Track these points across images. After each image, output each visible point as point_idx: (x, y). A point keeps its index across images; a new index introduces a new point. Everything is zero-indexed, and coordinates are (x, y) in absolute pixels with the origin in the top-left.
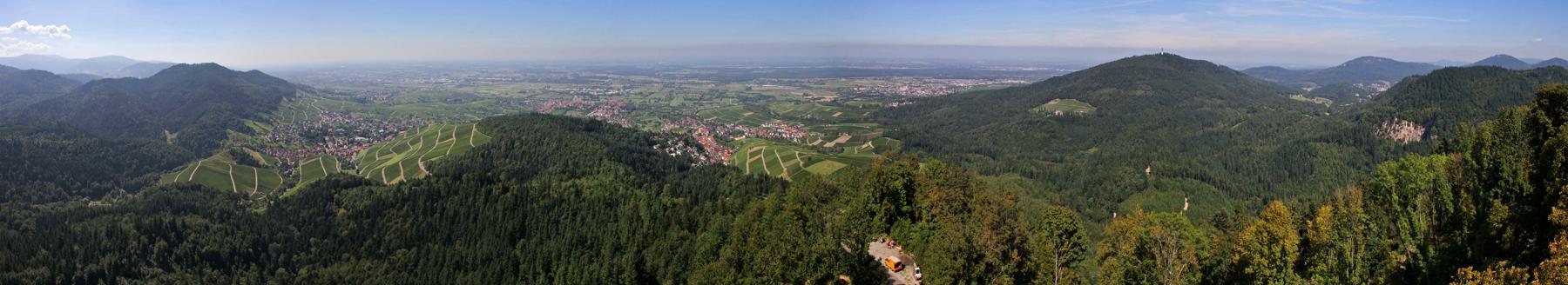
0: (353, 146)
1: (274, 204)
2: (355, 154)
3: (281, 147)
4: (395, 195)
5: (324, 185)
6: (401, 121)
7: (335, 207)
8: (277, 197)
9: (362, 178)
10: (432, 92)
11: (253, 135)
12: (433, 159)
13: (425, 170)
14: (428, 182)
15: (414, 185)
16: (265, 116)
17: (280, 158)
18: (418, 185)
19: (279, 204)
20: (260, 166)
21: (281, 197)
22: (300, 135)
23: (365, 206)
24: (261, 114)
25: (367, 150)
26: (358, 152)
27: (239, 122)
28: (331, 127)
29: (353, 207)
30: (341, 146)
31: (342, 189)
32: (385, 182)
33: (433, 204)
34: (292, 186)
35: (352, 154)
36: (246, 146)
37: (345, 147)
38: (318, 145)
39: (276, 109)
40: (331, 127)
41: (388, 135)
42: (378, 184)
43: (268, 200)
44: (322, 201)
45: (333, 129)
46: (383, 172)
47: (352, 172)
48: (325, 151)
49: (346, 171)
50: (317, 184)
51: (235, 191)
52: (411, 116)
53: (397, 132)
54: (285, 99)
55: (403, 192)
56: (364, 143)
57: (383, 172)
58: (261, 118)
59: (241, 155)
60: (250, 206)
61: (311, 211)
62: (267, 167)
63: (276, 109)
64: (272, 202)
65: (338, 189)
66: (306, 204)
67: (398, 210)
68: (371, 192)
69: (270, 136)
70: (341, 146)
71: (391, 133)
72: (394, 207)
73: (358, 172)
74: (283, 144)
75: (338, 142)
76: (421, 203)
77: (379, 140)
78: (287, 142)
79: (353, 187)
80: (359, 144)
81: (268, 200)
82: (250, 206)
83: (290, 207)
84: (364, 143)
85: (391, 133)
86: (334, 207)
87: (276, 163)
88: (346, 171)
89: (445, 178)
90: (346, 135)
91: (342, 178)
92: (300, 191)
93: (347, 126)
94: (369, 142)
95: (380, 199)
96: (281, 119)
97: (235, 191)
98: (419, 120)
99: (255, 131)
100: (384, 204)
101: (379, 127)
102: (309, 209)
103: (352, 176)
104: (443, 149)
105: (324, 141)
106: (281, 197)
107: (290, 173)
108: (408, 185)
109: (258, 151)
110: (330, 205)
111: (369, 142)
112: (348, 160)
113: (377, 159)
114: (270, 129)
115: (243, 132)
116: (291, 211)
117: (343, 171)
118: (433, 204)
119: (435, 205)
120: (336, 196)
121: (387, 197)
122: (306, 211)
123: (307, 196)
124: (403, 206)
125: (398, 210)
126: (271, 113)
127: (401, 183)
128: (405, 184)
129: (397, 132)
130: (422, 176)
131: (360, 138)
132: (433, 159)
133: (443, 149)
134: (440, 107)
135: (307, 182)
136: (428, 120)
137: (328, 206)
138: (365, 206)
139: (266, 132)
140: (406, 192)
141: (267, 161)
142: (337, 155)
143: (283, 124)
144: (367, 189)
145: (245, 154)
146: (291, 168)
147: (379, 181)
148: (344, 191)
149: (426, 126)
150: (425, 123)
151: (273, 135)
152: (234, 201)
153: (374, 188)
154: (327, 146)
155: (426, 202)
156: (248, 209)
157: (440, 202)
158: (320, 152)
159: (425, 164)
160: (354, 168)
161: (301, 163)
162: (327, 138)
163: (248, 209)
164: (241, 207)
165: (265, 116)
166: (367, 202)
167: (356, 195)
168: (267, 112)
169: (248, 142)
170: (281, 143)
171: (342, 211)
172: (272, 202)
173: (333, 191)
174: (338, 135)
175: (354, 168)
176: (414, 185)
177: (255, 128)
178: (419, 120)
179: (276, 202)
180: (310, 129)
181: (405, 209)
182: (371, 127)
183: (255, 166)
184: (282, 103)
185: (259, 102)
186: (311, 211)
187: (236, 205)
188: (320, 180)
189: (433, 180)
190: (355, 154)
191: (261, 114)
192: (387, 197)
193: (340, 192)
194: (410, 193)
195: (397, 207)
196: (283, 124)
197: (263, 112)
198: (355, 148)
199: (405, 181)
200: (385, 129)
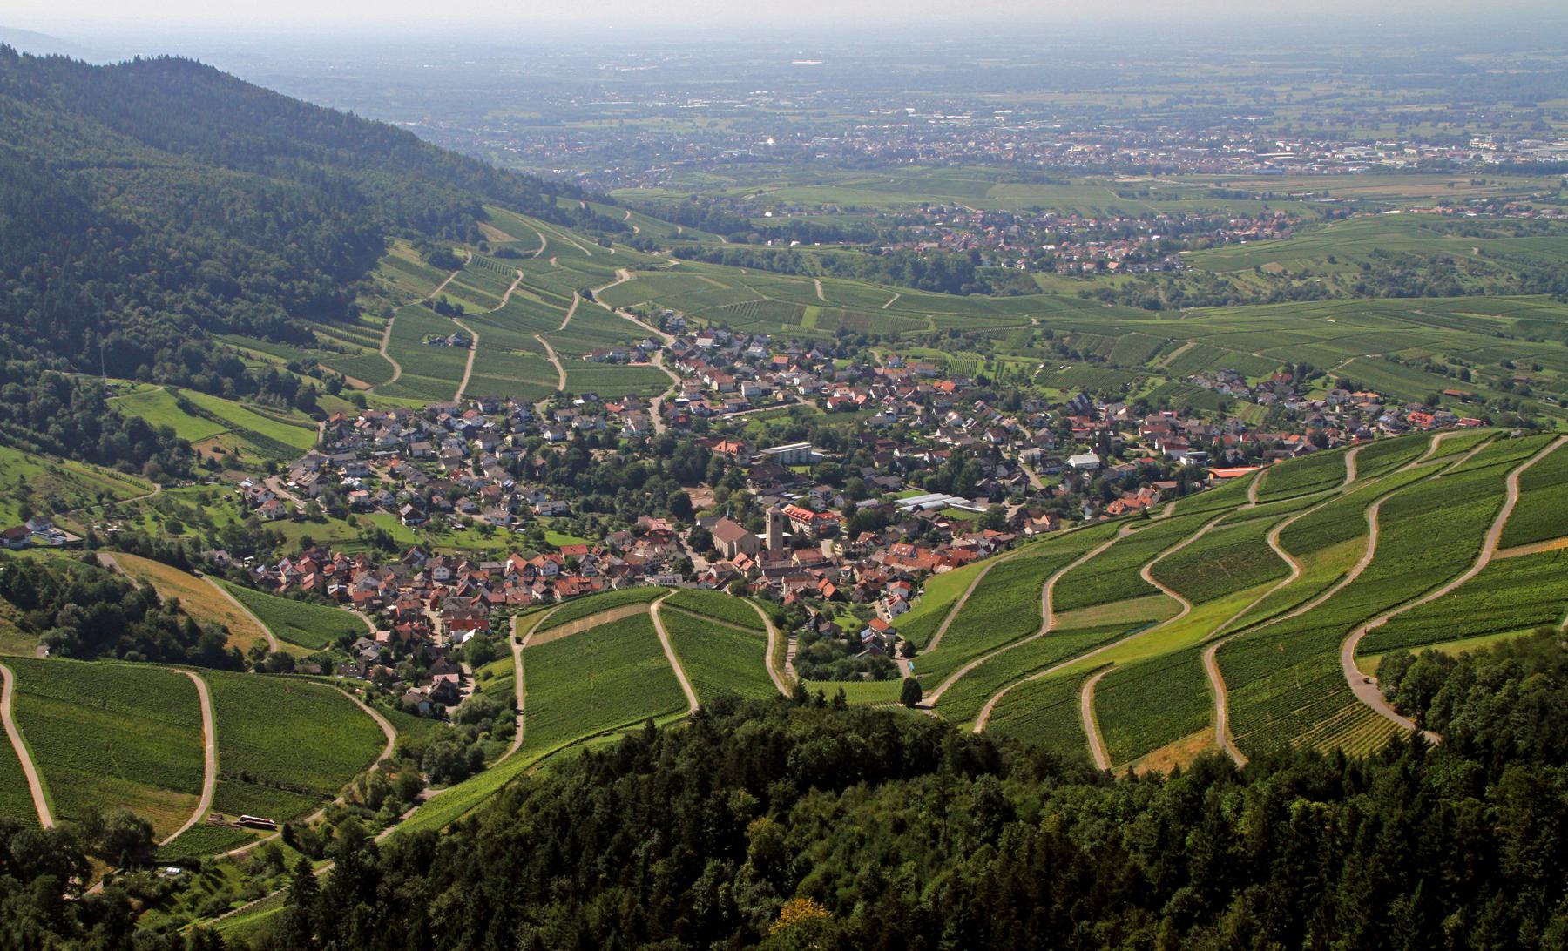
0: (881, 542)
1: (340, 879)
2: (895, 590)
3: (386, 543)
4: (1165, 837)
5: (682, 764)
6: (1224, 408)
7: (750, 889)
8: (358, 839)
9: (941, 729)
10: (1470, 230)
11: (174, 473)
12: (1452, 649)
13: (1387, 712)
14: (1411, 781)
15: (1300, 787)
16: (262, 359)
17: (373, 609)
18: (1333, 791)
19: (373, 877)
20: (234, 663)
21: (383, 838)
22: (514, 471)
23: (958, 890)
24: (227, 346)
25: (975, 572)
26: (913, 583)
27: (63, 391)
28: (728, 433)
29: (875, 890)
30: (801, 543)
31: (802, 789)
32: (1101, 763)
33: (1432, 911)
34: (457, 770)
35: (872, 592)
36: (117, 543)
37: (827, 548)
38: (639, 534)
39: (344, 313)
40: (728, 433)
41: (1131, 485)
42: (1048, 769)
43: (292, 858)
44: (664, 851)
45: (748, 444)
46: (1086, 697)
47: (865, 694)
48: (686, 568)
49: (830, 689)
50: (634, 755)
51: (47, 820)
52: (1302, 376)
53: (1197, 473)
54: (403, 250)
55: (1225, 826)
56: (962, 527)
57: (1086, 697)
58: (233, 368)
59: (79, 597)
60: (162, 900)
61: (594, 911)
62: (284, 664)
63: (341, 312)
64: (323, 870)
65: (776, 788)
66: (556, 866)
67: (1181, 923)
68: (998, 812)
69: (302, 474)
70: (801, 543)
71: (1151, 475)
72: (1155, 904)
73: (912, 694)
74: (402, 532)
75: (783, 522)
76: (1345, 898)
77: (1062, 511)
78: (423, 511)
79: (875, 776)
80: (925, 531)
81: (292, 858)
82: (162, 900)
83: (455, 890)
84: (962, 527)
85: (1151, 475)
86: (745, 887)
87: (347, 643)
88: (830, 689)
89: (1541, 770)
90: (833, 478)
91: (796, 730)
92: (516, 796)
93: (844, 427)
94: (994, 522)
95: (1059, 852)
96: (377, 373)
97: (47, 820)
98: (1365, 402)
99: (186, 447)
100: (1087, 877)
101: (1065, 438)
102: (585, 895)
103: (867, 720)
104: (1536, 591)
105: (683, 511)
106: (383, 838)
107: (449, 695)
108: (1264, 788)
109: (217, 571)
110: (720, 877)
111: (994, 522)
112: (846, 622)
113: (1050, 622)
114: (305, 436)
115: (92, 457)
116: (457, 907)
117: (812, 687)
118: (1432, 911)
119: (1453, 920)
120: (762, 825)
121: (1112, 848)
122: (556, 910)
123: (563, 822)
124: (1220, 903)
125: (1181, 923)
126: (307, 340)
127: (1211, 771)
128: (1239, 778)
129: (1197, 473)
130: (1362, 744)
131: (931, 500)
132: (1452, 649)
133: (1536, 591)
134: (1529, 326)
135: (563, 748)
136: (1433, 402)
137: (700, 886)
138: (958, 890)
139: (277, 458)
140: (1243, 827)
141: (287, 627)
142: (769, 595)
143: (389, 405)
144: (971, 792)
145: (114, 593)
146: (453, 665)
147: (1056, 749)
148: (816, 803)
149: (1410, 441)
150: (1401, 425)
151: (326, 475)
152: (43, 880)
153: (1017, 792)
154: (703, 543)
155: (1379, 899)
156: (149, 921)
157: (1489, 911)
158: (653, 569)
159: (1392, 675)
160: (884, 671)
161: (523, 636)
162: (702, 498)
163: (149, 921)
164: (92, 912)
165: (262, 359)
166: (973, 868)
167: (900, 827)
168: (279, 334)
169: (133, 513)
170: (381, 520)
171: (800, 910)
172: (323, 870)
173: (742, 797)
174: (778, 477)
175: (884, 671)
176: (1300, 787)
177: (188, 429)
178: (1365, 402)
179: (347, 859)
180: (584, 444)
181: (1228, 923)
182: (1008, 434)
183: (197, 662)
184: (383, 276)
185: (208, 268)
186: (594, 911)
187: (52, 901)
188: (651, 731)
189: (1445, 774)
190: (895, 590)
191: (227, 346)
192: (1112, 848)
193: (788, 802)
194: (1269, 832)
195: (1170, 905)
196: (389, 405)
197: (246, 329)
198: (896, 556)
199: (1240, 761)
200: (1105, 447)
